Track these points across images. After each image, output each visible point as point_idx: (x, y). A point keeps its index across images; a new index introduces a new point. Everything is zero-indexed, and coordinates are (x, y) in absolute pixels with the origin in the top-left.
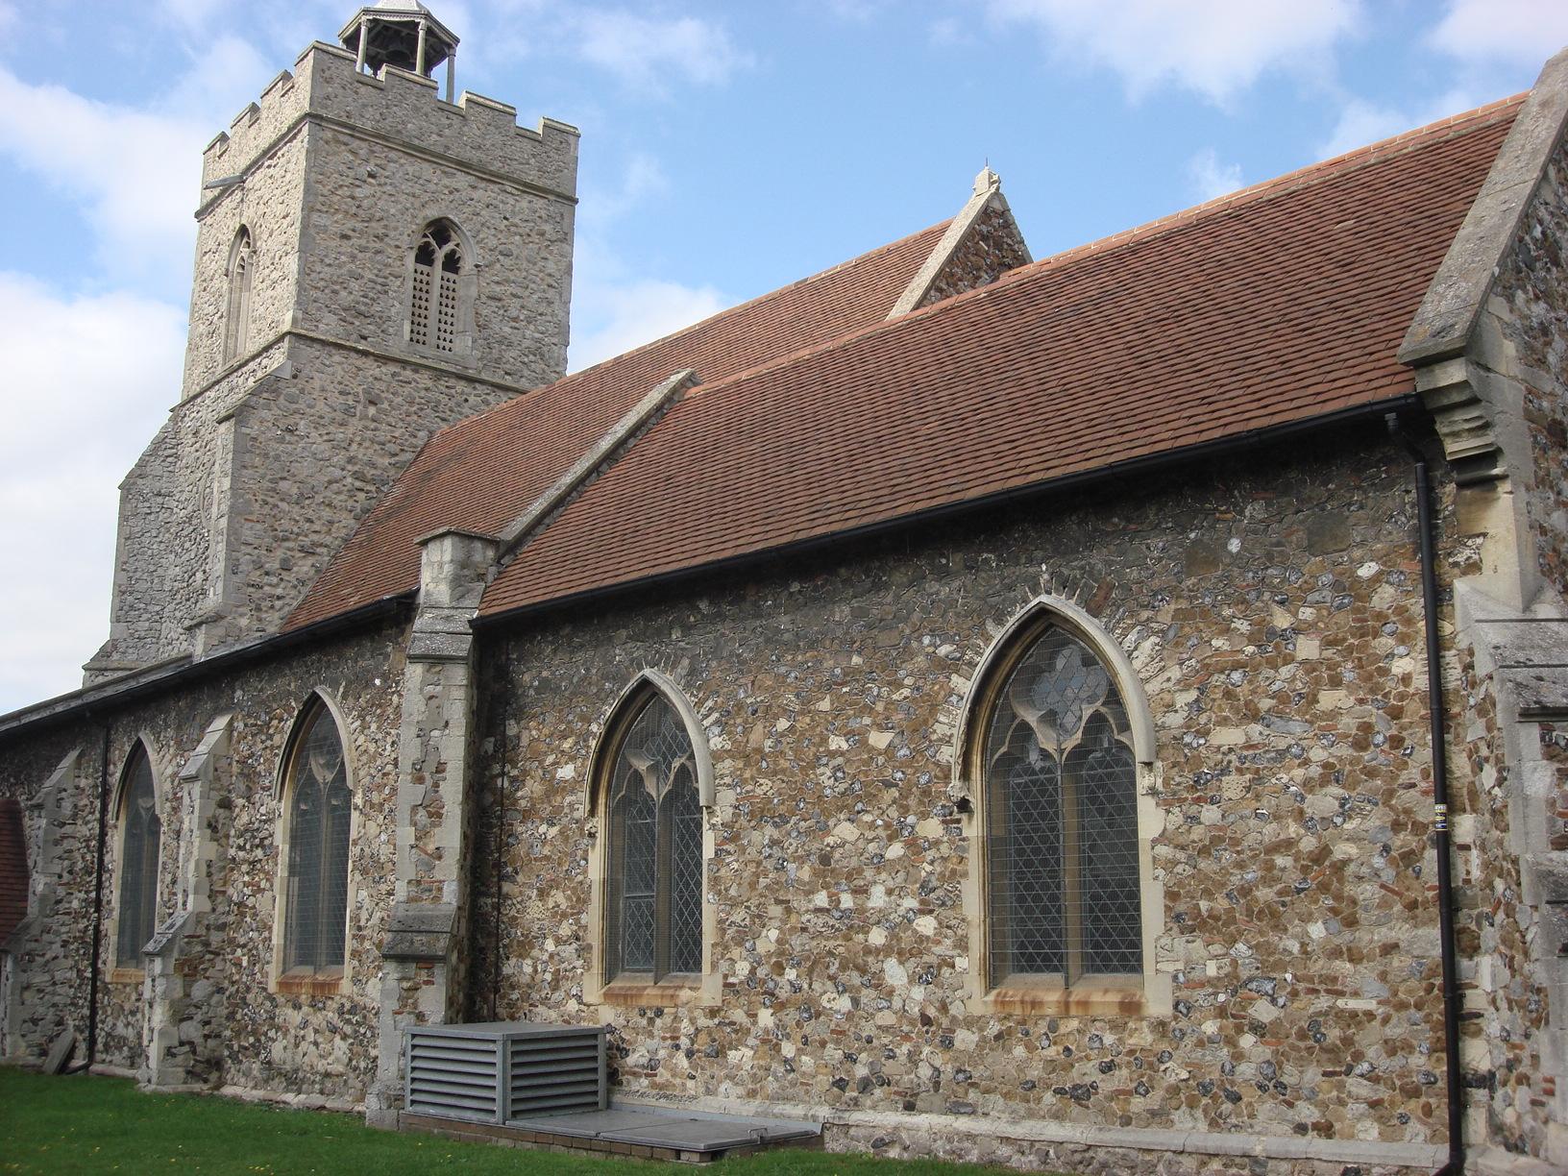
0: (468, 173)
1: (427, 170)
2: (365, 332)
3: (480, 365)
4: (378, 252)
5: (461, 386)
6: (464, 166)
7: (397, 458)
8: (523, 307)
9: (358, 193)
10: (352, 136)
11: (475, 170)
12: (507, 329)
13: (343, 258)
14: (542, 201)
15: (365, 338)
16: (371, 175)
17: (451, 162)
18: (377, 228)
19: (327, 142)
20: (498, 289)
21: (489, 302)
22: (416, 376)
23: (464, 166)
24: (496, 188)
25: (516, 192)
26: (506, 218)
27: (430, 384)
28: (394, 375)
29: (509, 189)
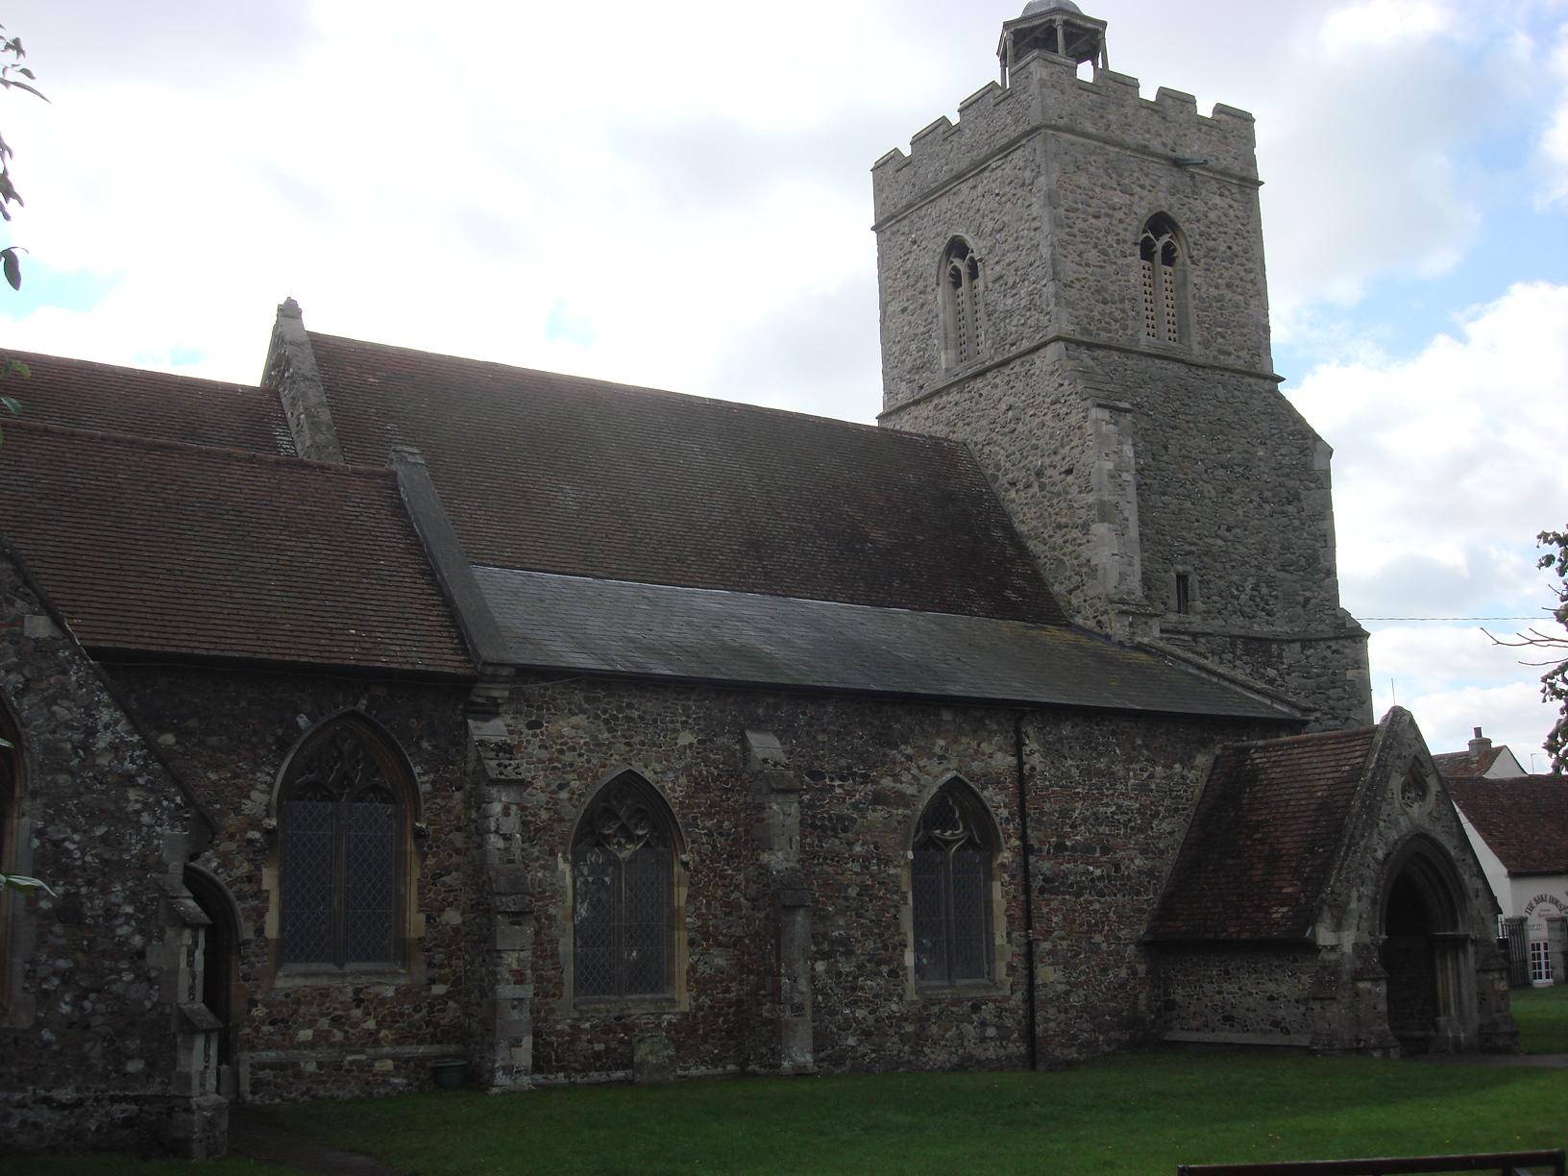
0: (968, 179)
1: (944, 203)
2: (921, 382)
3: (993, 351)
4: (923, 305)
5: (979, 383)
6: (959, 177)
7: (1070, 446)
8: (1016, 270)
9: (909, 265)
10: (898, 221)
11: (969, 172)
12: (1009, 301)
13: (905, 329)
14: (1019, 151)
15: (921, 387)
16: (914, 242)
17: (951, 183)
18: (920, 285)
19: (889, 240)
20: (998, 268)
21: (997, 285)
22: (950, 398)
23: (959, 177)
24: (986, 174)
25: (999, 163)
26: (997, 195)
27: (957, 397)
28: (935, 407)
29: (994, 165)
